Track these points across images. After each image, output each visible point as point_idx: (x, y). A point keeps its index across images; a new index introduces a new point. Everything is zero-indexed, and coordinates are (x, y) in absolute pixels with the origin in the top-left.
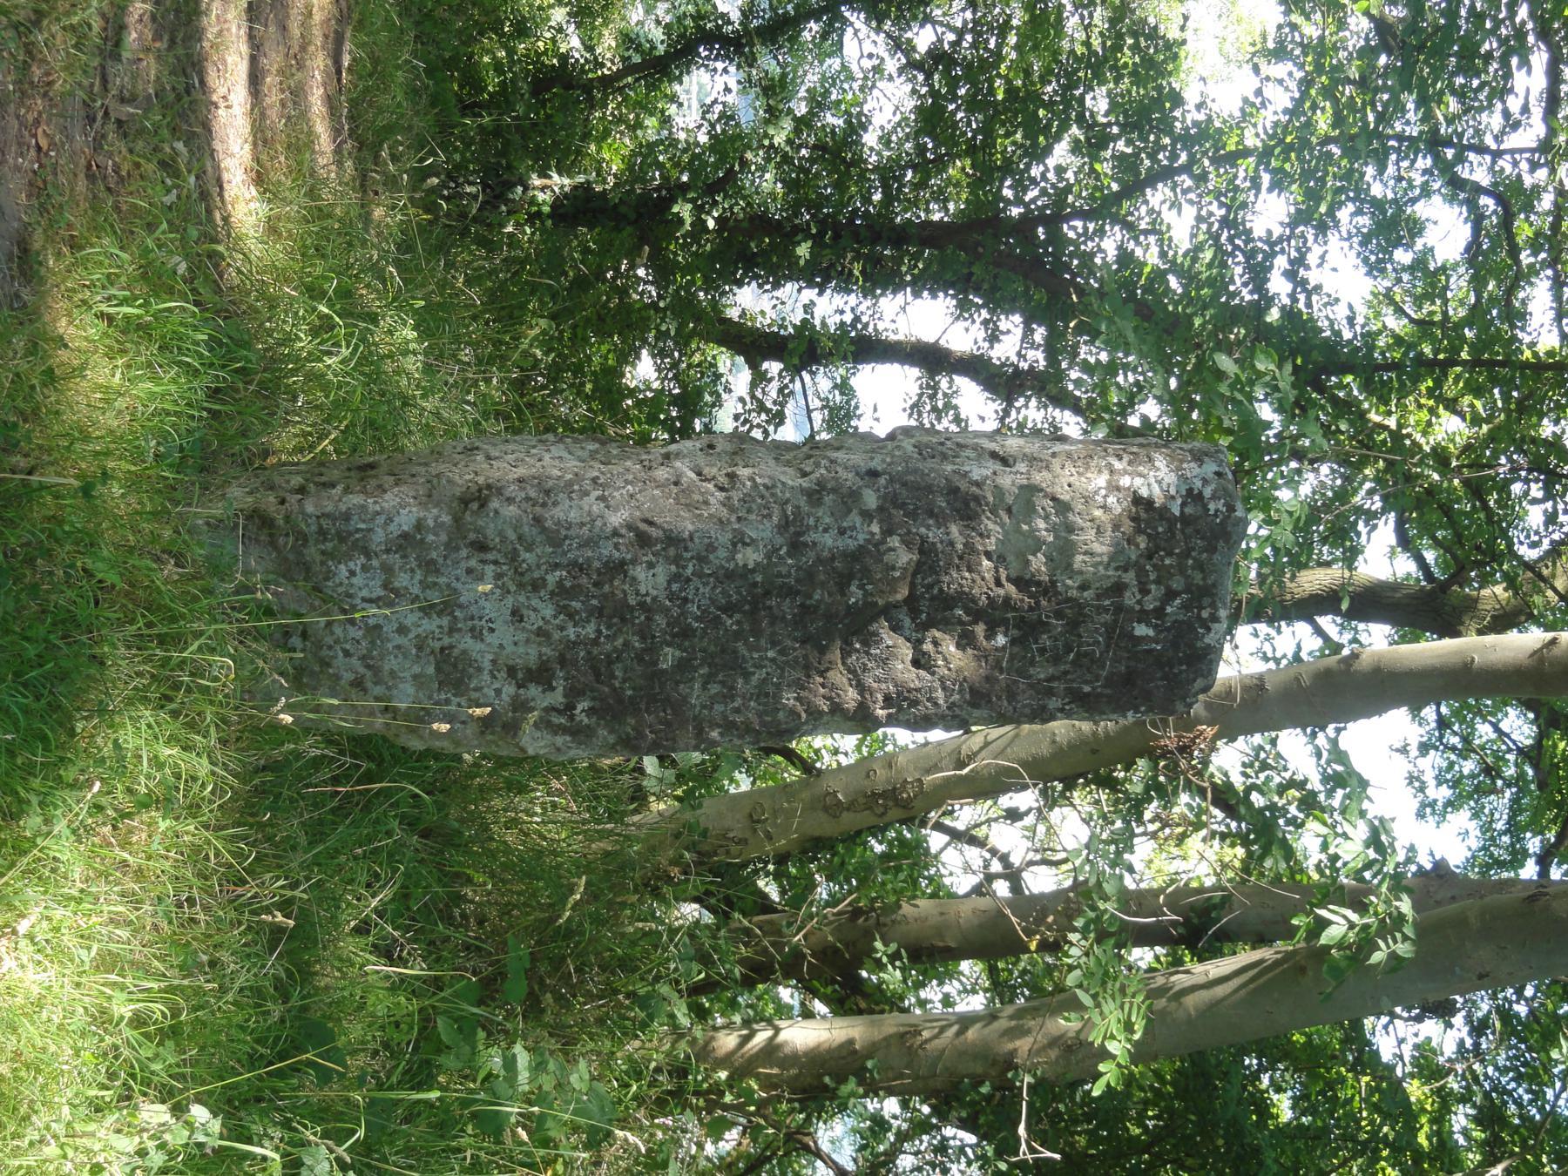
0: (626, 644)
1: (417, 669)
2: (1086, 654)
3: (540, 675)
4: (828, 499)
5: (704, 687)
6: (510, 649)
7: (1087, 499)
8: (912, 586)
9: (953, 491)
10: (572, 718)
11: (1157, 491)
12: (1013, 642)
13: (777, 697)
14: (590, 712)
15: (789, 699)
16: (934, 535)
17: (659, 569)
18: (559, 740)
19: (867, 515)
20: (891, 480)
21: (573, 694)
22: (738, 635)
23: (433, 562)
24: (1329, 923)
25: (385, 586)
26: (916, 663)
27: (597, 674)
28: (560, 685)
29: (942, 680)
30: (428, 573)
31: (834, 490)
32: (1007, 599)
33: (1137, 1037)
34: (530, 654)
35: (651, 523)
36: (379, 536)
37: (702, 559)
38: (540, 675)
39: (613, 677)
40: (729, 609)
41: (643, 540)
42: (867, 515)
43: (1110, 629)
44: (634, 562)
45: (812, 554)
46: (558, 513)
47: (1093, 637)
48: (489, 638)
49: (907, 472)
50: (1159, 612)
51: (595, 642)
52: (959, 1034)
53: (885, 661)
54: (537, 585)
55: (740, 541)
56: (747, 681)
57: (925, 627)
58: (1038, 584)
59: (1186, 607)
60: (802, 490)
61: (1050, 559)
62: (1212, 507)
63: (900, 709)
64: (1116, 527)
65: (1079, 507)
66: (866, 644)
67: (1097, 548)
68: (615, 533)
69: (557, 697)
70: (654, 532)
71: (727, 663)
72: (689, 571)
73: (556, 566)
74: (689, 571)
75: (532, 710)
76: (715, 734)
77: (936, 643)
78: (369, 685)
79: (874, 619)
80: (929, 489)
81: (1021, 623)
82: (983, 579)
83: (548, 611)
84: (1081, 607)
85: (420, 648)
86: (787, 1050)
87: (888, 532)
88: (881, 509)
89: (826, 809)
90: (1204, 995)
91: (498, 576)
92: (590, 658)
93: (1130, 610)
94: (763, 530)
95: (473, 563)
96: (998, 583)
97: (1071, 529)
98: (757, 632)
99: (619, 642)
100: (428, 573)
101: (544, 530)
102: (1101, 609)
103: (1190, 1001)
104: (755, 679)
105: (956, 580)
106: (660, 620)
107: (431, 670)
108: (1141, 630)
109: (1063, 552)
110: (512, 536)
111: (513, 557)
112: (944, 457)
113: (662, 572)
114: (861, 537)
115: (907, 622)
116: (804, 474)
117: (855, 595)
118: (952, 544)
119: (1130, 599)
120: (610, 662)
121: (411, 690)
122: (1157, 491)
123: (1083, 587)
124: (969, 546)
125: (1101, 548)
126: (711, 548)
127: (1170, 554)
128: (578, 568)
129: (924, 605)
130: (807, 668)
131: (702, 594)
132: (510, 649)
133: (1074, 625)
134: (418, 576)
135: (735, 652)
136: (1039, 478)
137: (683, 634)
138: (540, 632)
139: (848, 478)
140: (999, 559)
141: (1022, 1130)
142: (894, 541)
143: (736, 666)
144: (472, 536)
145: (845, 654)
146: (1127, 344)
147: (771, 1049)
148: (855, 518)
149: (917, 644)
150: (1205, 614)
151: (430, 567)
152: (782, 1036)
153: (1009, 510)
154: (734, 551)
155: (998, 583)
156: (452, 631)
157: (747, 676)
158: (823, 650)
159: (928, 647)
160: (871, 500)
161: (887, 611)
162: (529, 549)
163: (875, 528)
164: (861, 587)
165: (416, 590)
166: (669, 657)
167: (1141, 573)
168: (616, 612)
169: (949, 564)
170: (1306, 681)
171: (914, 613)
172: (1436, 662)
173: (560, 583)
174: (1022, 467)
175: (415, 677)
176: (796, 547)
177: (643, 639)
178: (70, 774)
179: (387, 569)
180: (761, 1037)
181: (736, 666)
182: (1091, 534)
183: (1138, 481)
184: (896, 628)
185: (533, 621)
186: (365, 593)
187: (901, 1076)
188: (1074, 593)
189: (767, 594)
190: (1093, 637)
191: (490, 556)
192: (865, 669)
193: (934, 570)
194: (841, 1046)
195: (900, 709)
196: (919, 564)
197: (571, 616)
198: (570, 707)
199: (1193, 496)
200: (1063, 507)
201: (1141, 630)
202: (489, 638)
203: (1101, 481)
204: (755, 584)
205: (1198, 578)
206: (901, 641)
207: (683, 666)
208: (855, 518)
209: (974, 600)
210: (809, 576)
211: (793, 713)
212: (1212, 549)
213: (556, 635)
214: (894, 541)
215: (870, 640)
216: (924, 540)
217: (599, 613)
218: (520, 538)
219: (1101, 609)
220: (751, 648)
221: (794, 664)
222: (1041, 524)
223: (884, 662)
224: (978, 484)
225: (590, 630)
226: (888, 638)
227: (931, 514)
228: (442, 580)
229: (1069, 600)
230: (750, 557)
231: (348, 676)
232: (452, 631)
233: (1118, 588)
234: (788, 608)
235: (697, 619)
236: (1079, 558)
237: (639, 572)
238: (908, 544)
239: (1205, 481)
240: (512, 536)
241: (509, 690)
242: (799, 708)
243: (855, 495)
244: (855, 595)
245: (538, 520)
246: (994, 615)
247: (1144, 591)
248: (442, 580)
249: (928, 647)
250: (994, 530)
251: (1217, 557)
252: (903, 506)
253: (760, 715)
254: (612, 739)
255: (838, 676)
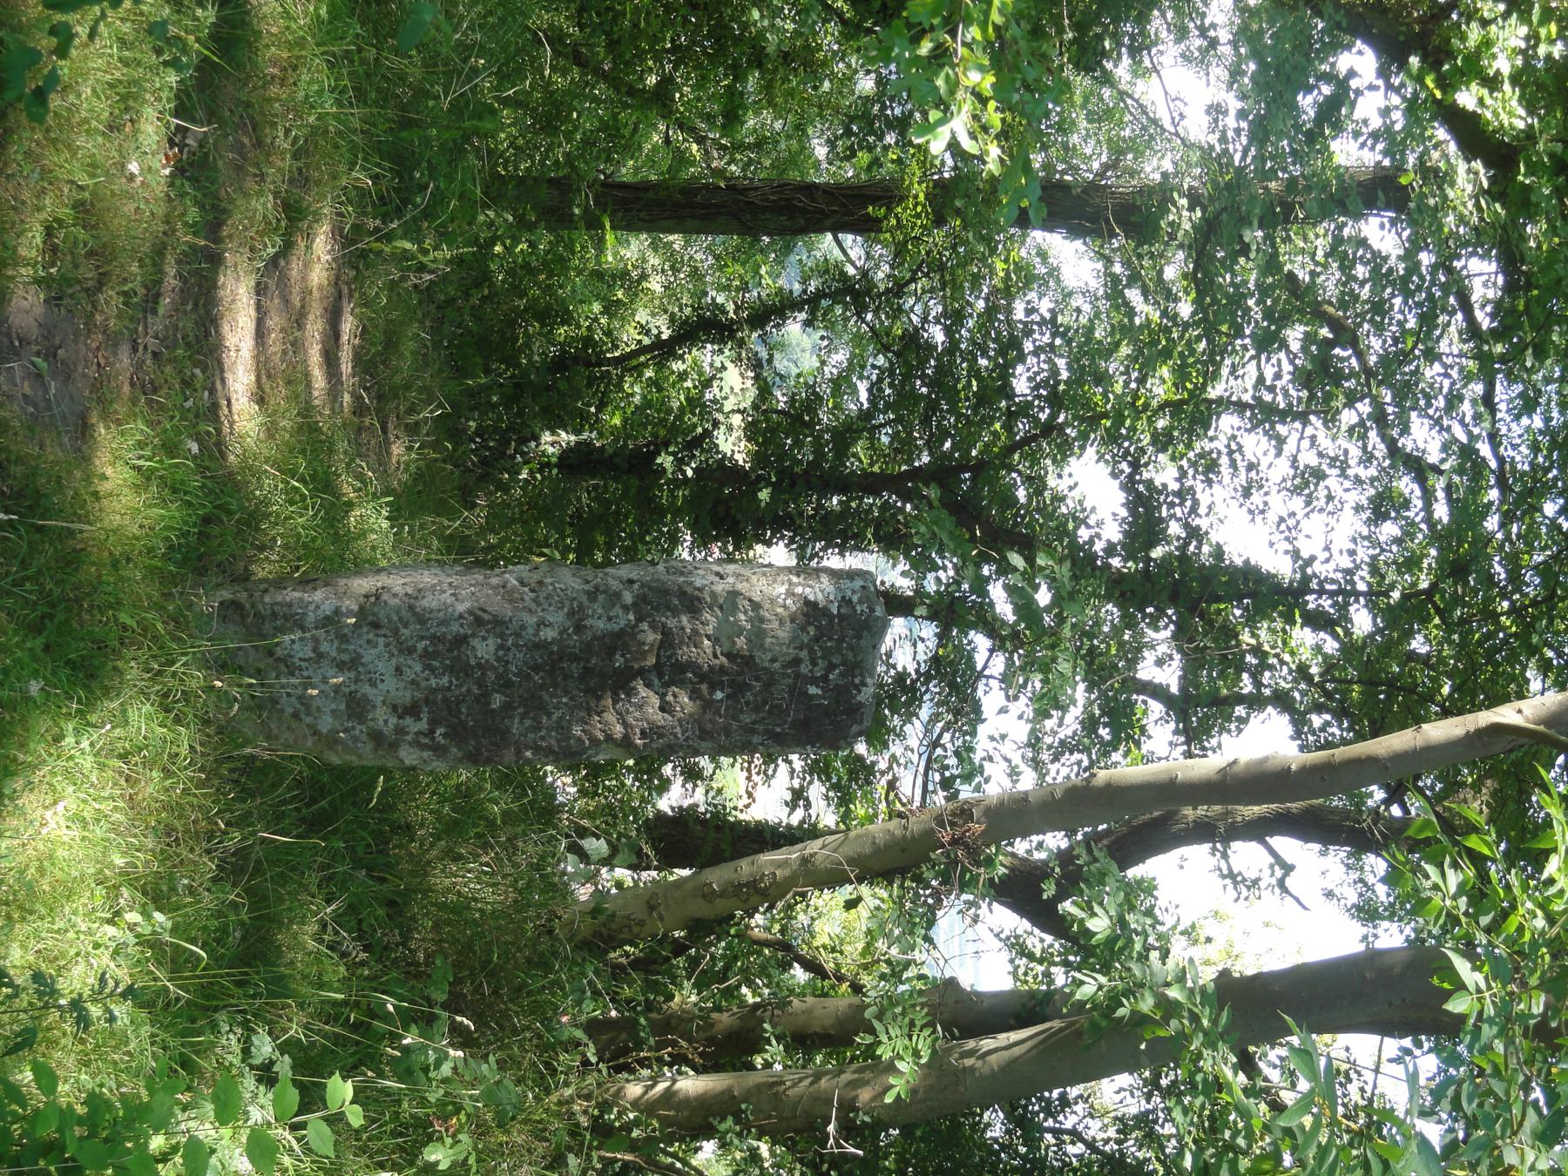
0: (469, 690)
1: (333, 706)
2: (777, 706)
3: (412, 710)
4: (601, 597)
5: (521, 722)
6: (393, 693)
7: (772, 601)
8: (658, 657)
9: (682, 594)
10: (433, 739)
11: (820, 596)
12: (728, 697)
13: (569, 729)
14: (445, 735)
15: (577, 731)
16: (671, 623)
17: (490, 641)
18: (425, 754)
19: (626, 608)
20: (642, 586)
21: (433, 723)
22: (543, 687)
23: (345, 635)
24: (1082, 983)
25: (314, 650)
26: (662, 709)
27: (450, 711)
28: (425, 716)
29: (680, 720)
30: (342, 642)
31: (604, 592)
32: (722, 666)
33: (923, 1061)
34: (406, 697)
35: (484, 611)
36: (311, 617)
37: (518, 635)
38: (412, 710)
39: (460, 712)
40: (536, 668)
41: (479, 622)
42: (626, 608)
43: (792, 689)
44: (473, 635)
45: (589, 633)
46: (424, 603)
47: (780, 693)
48: (380, 686)
49: (652, 580)
50: (825, 678)
51: (449, 689)
52: (812, 1083)
53: (641, 707)
54: (411, 651)
55: (542, 623)
56: (549, 718)
57: (667, 685)
58: (742, 657)
59: (842, 675)
60: (586, 592)
61: (749, 641)
62: (858, 608)
63: (652, 740)
64: (792, 621)
65: (767, 606)
66: (628, 695)
67: (780, 633)
68: (461, 616)
69: (423, 725)
70: (486, 617)
71: (535, 706)
72: (510, 643)
73: (423, 638)
74: (510, 643)
75: (407, 733)
76: (528, 754)
77: (675, 696)
78: (303, 716)
79: (634, 678)
80: (667, 592)
81: (732, 684)
82: (705, 653)
83: (418, 668)
84: (772, 674)
85: (336, 692)
86: (681, 1095)
87: (640, 619)
88: (634, 604)
89: (704, 896)
90: (1006, 1054)
91: (387, 645)
92: (446, 700)
93: (805, 676)
94: (557, 617)
95: (371, 636)
96: (715, 656)
97: (762, 620)
98: (555, 686)
99: (464, 689)
100: (342, 642)
101: (415, 614)
102: (785, 675)
103: (992, 1058)
104: (554, 717)
105: (686, 653)
106: (491, 676)
107: (343, 707)
108: (813, 690)
109: (758, 635)
110: (395, 618)
111: (396, 632)
112: (682, 574)
113: (492, 643)
114: (622, 623)
115: (656, 681)
116: (588, 582)
117: (619, 662)
118: (683, 628)
119: (804, 669)
120: (458, 704)
121: (330, 720)
122: (820, 596)
123: (773, 660)
124: (695, 632)
125: (784, 634)
126: (523, 627)
127: (830, 639)
128: (435, 639)
129: (667, 670)
130: (589, 710)
131: (518, 658)
132: (393, 693)
133: (767, 686)
134: (336, 644)
135: (541, 698)
136: (739, 586)
137: (505, 685)
138: (413, 682)
139: (615, 585)
140: (716, 640)
141: (831, 1128)
142: (645, 626)
143: (542, 708)
144: (370, 618)
145: (615, 702)
146: (942, 544)
147: (669, 1094)
148: (618, 610)
149: (662, 696)
150: (857, 681)
151: (343, 639)
152: (678, 1085)
153: (721, 608)
154: (538, 630)
155: (715, 656)
156: (357, 680)
157: (549, 715)
158: (599, 698)
159: (670, 698)
160: (628, 598)
161: (641, 673)
162: (406, 627)
163: (631, 617)
164: (623, 656)
165: (334, 654)
166: (497, 701)
167: (811, 652)
168: (461, 669)
169: (682, 642)
170: (1058, 794)
171: (660, 675)
172: (1151, 778)
173: (425, 649)
174: (731, 580)
175: (333, 711)
176: (579, 628)
177: (480, 687)
178: (93, 718)
179: (316, 640)
180: (661, 1087)
181: (542, 708)
182: (775, 625)
183: (808, 590)
184: (648, 685)
185: (409, 675)
186: (300, 655)
187: (770, 1117)
188: (767, 665)
189: (561, 659)
190: (780, 693)
191: (382, 632)
192: (628, 712)
193: (671, 646)
194: (723, 1092)
195: (652, 740)
196: (662, 642)
197: (433, 671)
198: (432, 732)
199: (845, 601)
200: (756, 606)
201: (813, 690)
202: (380, 686)
203: (782, 589)
204: (552, 653)
205: (850, 656)
206: (651, 693)
207: (507, 707)
208: (618, 610)
209: (700, 667)
210: (588, 648)
211: (579, 739)
212: (860, 637)
213: (424, 684)
214: (645, 626)
215: (631, 692)
216: (664, 625)
217: (451, 669)
218: (400, 619)
219: (785, 675)
220: (552, 696)
221: (580, 707)
222: (743, 617)
223: (640, 707)
224: (699, 589)
225: (445, 681)
226: (643, 692)
227: (669, 609)
228: (351, 647)
229: (764, 669)
230: (549, 634)
231: (290, 710)
232: (357, 680)
233: (796, 662)
234: (575, 669)
235: (515, 675)
236: (769, 640)
237: (475, 642)
238: (653, 627)
239: (854, 592)
240: (395, 618)
241: (393, 721)
242: (584, 737)
243: (618, 595)
244: (619, 662)
245: (411, 607)
246: (712, 678)
247: (814, 664)
248: (351, 647)
249: (670, 698)
250: (711, 620)
251: (863, 642)
252: (650, 603)
253: (558, 741)
254: (460, 754)
255: (610, 717)
